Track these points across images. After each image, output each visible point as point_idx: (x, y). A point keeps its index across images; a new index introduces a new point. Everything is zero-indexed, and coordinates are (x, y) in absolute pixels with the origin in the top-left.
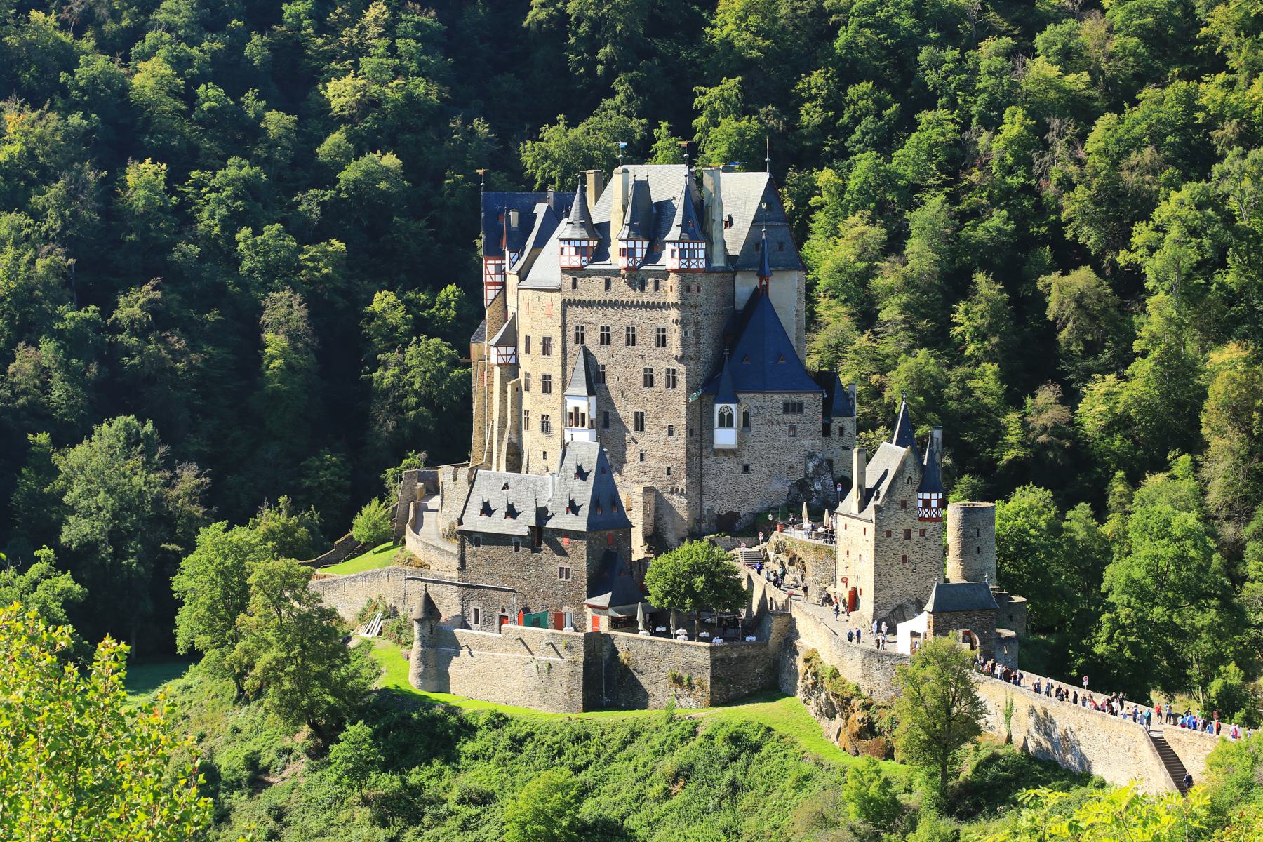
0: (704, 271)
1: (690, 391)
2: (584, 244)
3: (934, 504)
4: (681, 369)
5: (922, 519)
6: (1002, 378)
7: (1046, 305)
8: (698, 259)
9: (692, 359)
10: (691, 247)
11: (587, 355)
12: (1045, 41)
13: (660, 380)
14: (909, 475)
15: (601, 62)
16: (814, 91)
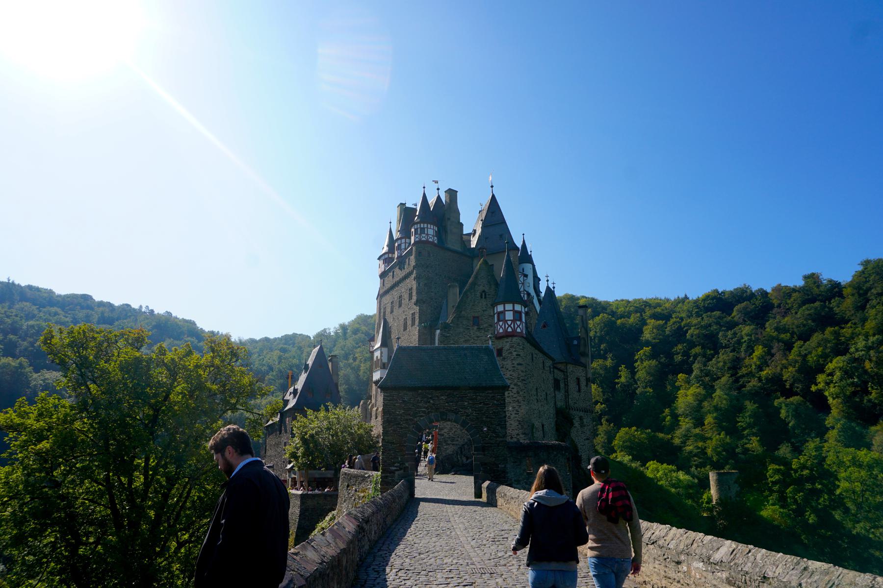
0: (435, 245)
1: (420, 323)
2: (386, 256)
3: (509, 316)
4: (417, 309)
5: (499, 337)
6: (762, 442)
7: (780, 413)
8: (427, 234)
9: (424, 302)
10: (422, 226)
11: (386, 323)
12: (770, 325)
13: (409, 322)
14: (481, 288)
15: (602, 350)
16: (678, 351)
